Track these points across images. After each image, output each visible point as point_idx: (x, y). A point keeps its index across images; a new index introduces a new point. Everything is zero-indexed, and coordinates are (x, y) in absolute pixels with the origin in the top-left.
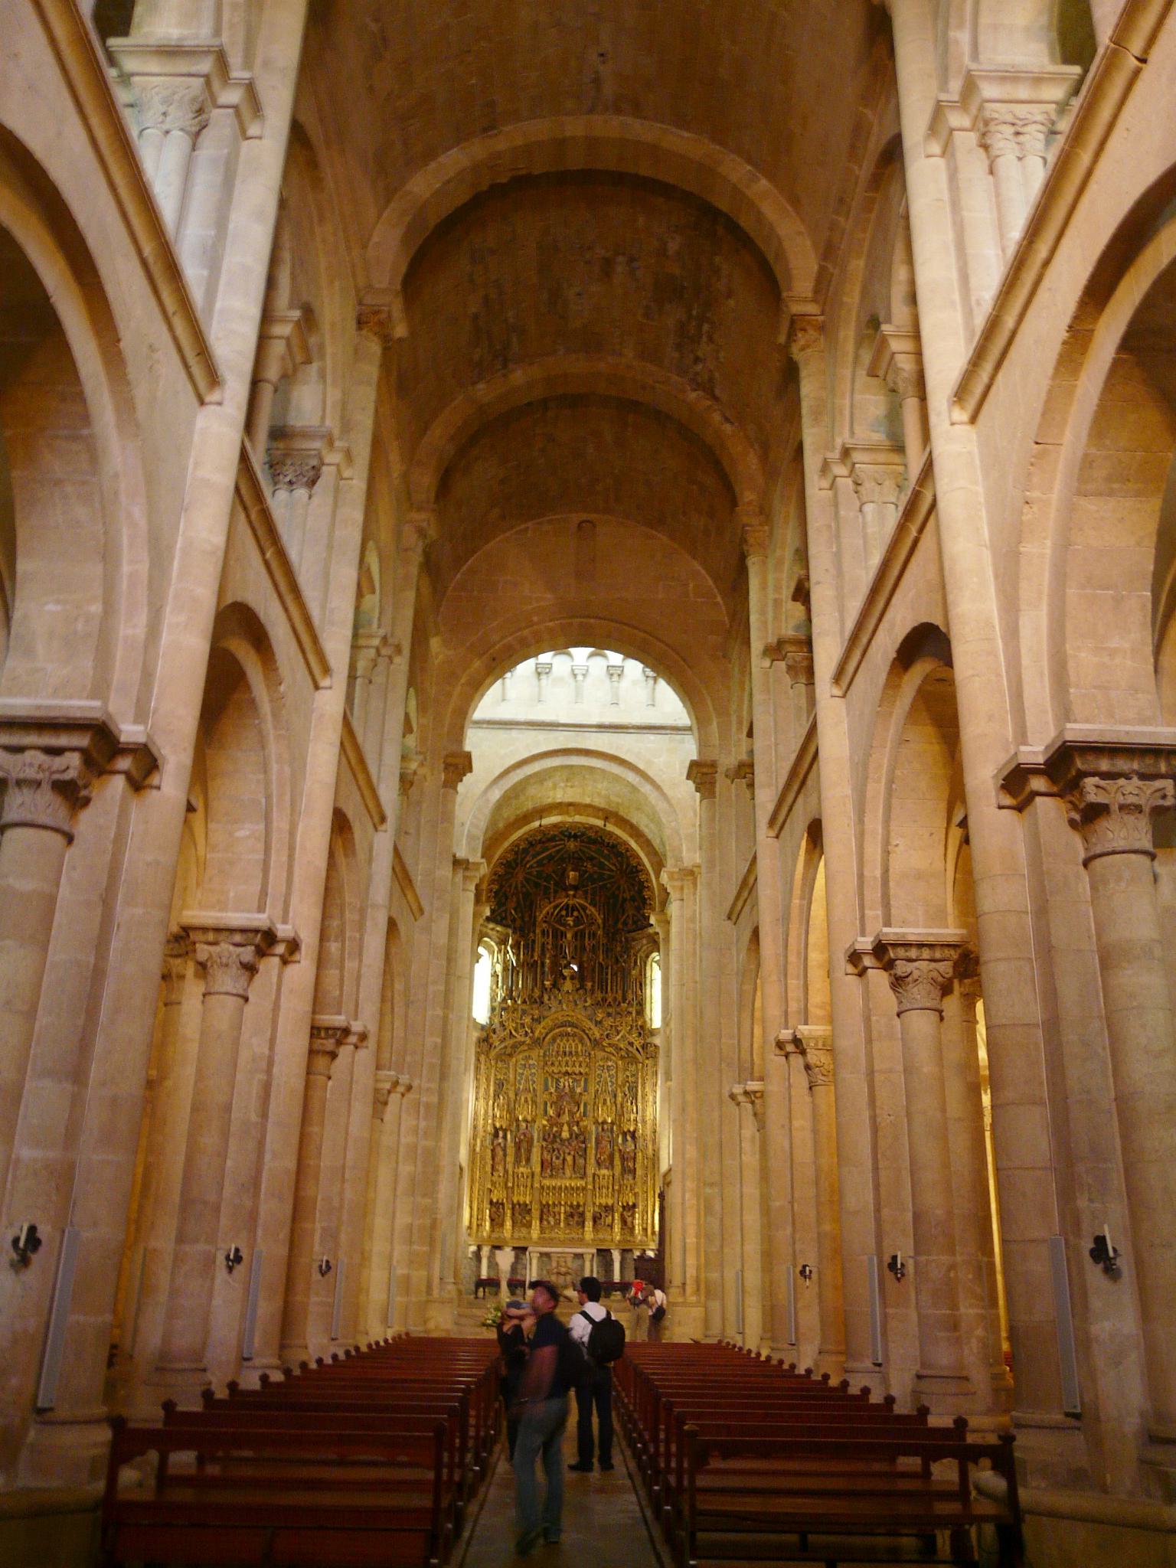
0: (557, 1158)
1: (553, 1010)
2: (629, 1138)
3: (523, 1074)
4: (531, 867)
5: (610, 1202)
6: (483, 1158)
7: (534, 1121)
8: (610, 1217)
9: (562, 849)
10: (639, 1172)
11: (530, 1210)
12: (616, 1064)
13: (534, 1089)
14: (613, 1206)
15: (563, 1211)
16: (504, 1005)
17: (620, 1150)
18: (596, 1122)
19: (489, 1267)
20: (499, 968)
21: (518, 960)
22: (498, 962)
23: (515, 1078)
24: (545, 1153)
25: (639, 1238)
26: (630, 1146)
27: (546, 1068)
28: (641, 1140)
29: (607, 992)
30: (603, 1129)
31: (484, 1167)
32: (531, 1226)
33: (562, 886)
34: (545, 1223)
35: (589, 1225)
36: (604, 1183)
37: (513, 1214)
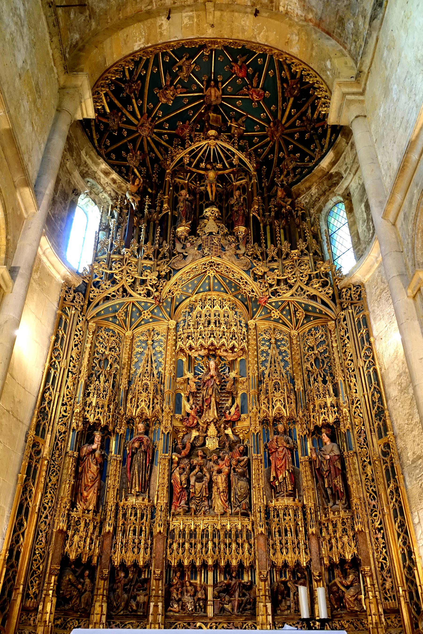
0: (199, 479)
1: (190, 258)
3: (142, 353)
11: (147, 581)
13: (159, 373)
14: (308, 567)
15: (210, 581)
17: (311, 462)
20: (112, 223)
23: (130, 358)
27: (179, 343)
29: (266, 247)
31: (57, 487)
37: (111, 590)
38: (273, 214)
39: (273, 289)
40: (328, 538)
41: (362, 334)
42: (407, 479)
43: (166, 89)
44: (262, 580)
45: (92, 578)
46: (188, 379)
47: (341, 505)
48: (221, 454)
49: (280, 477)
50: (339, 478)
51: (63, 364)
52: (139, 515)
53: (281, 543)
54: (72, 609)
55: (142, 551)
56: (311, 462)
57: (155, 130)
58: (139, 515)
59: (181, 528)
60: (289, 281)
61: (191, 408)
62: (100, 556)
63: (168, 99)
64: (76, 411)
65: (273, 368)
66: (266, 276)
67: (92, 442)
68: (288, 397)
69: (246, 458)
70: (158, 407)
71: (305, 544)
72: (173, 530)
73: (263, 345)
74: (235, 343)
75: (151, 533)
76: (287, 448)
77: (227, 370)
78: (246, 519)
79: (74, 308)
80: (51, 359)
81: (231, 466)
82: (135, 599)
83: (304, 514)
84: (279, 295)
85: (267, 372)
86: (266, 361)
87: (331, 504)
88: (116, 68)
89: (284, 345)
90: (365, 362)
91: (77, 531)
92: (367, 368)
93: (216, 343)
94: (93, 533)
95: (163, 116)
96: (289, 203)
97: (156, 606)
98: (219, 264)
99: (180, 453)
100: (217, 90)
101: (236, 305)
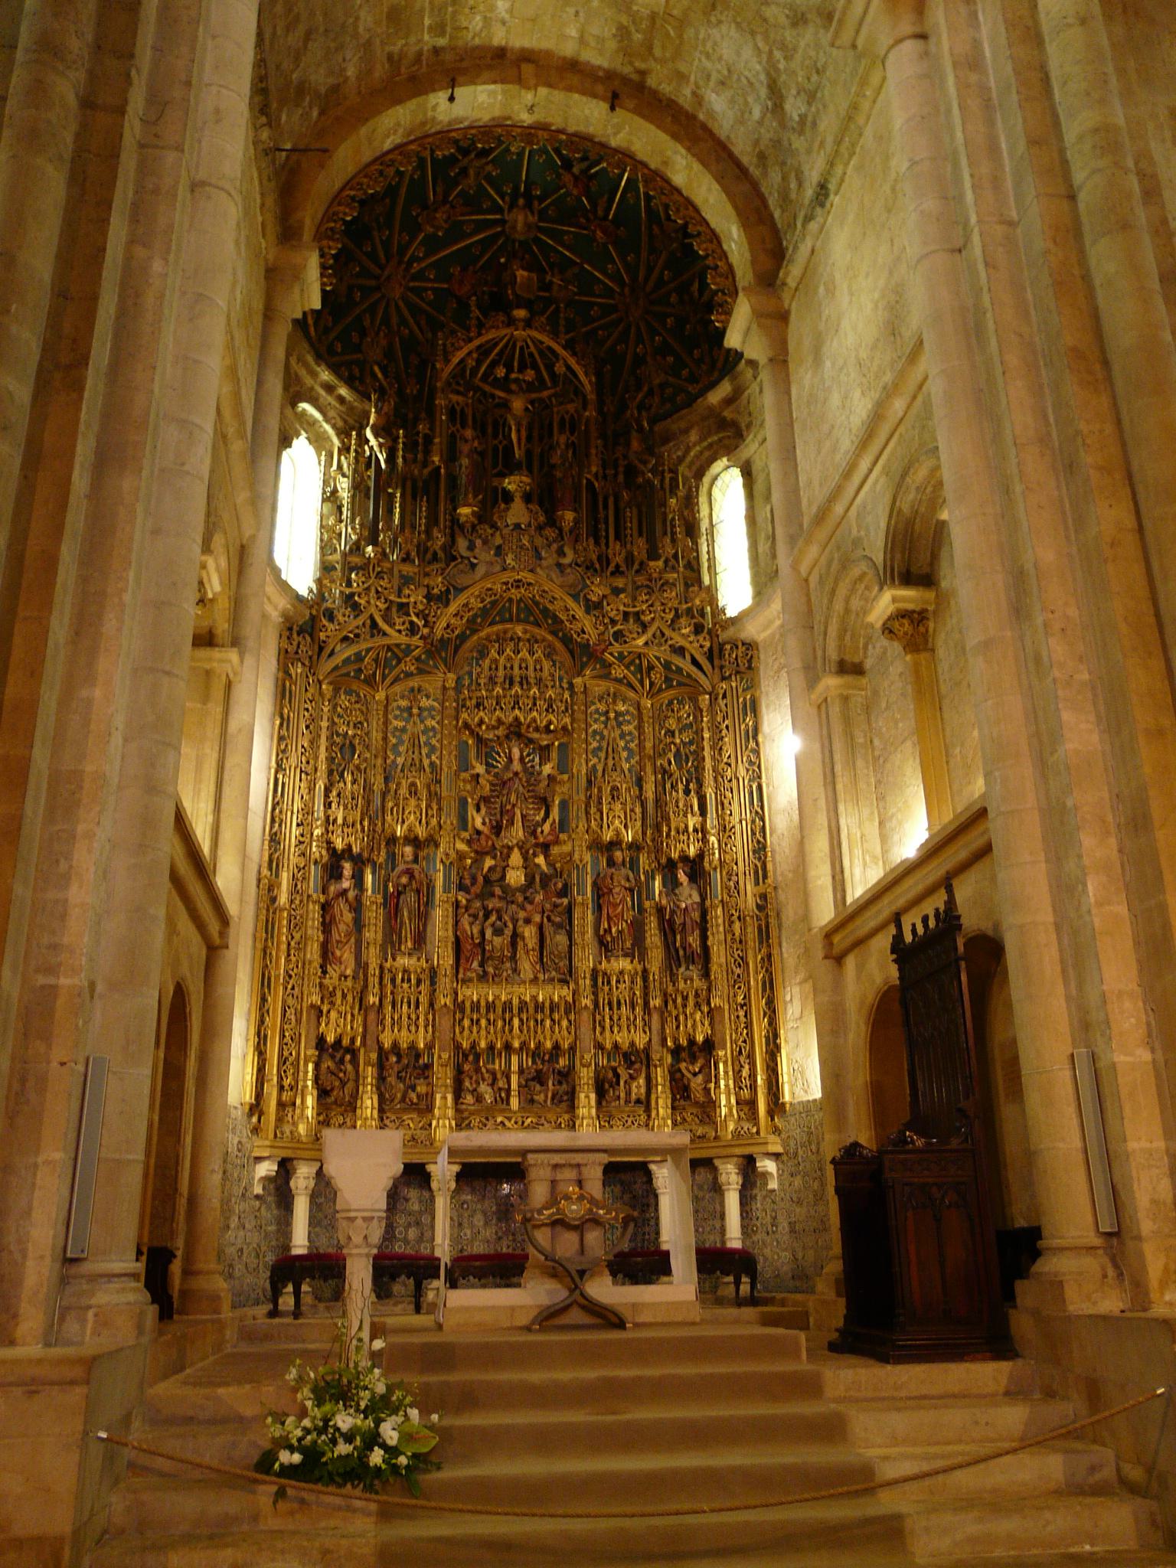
0: (498, 932)
1: (481, 570)
2: (682, 877)
3: (403, 730)
4: (420, 276)
5: (641, 1040)
6: (295, 924)
7: (432, 841)
8: (642, 1081)
9: (497, 236)
10: (719, 956)
11: (428, 1066)
12: (639, 708)
13: (432, 764)
14: (647, 1050)
15: (515, 1067)
16: (355, 560)
17: (660, 910)
18: (598, 846)
19: (313, 1222)
20: (344, 485)
21: (391, 459)
22: (340, 467)
23: (385, 739)
24: (465, 921)
25: (731, 1126)
26: (688, 895)
27: (464, 715)
28: (717, 877)
30: (611, 863)
32: (430, 1109)
33: (498, 304)
34: (469, 1099)
35: (587, 1102)
36: (622, 992)
37: (381, 1079)
38: (621, 478)
39: (616, 629)
40: (674, 1013)
41: (747, 725)
42: (784, 944)
43: (436, 210)
44: (584, 1066)
45: (355, 1062)
46: (478, 775)
47: (696, 971)
48: (528, 894)
49: (614, 930)
50: (697, 932)
51: (293, 761)
52: (413, 981)
53: (611, 1019)
54: (335, 1102)
55: (422, 1030)
56: (660, 910)
57: (412, 284)
58: (413, 981)
59: (475, 999)
60: (642, 617)
61: (484, 823)
62: (364, 1037)
63: (438, 228)
64: (315, 833)
65: (610, 762)
66: (605, 603)
67: (339, 877)
68: (632, 810)
69: (565, 901)
70: (434, 821)
71: (643, 1019)
72: (463, 1002)
73: (596, 721)
74: (553, 719)
75: (431, 1005)
76: (626, 888)
77: (537, 759)
78: (565, 987)
79: (300, 665)
80: (277, 755)
81: (543, 912)
82: (414, 1089)
83: (645, 979)
84: (625, 642)
85: (600, 768)
86: (600, 749)
87: (682, 970)
88: (352, 193)
89: (629, 722)
90: (748, 770)
91: (332, 1003)
92: (750, 780)
93: (522, 720)
94: (352, 1008)
95: (427, 255)
96: (650, 466)
97: (444, 1098)
98: (529, 584)
99: (468, 892)
100: (529, 214)
101: (554, 649)
